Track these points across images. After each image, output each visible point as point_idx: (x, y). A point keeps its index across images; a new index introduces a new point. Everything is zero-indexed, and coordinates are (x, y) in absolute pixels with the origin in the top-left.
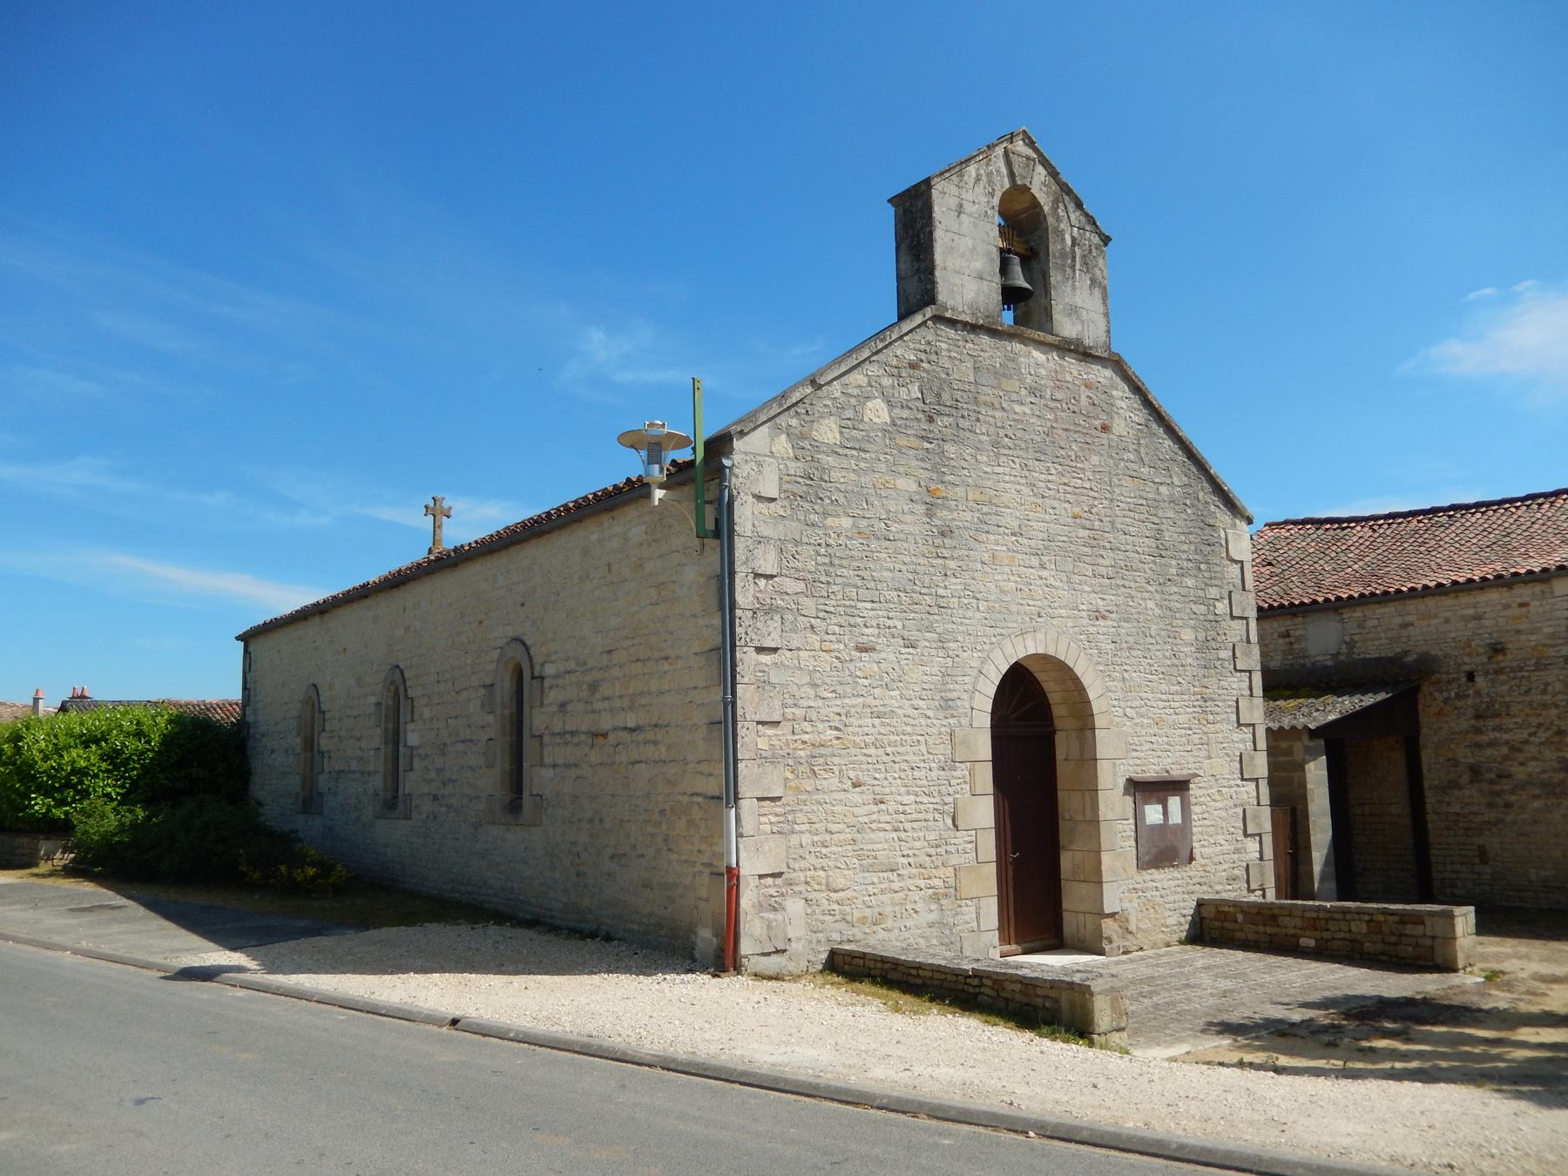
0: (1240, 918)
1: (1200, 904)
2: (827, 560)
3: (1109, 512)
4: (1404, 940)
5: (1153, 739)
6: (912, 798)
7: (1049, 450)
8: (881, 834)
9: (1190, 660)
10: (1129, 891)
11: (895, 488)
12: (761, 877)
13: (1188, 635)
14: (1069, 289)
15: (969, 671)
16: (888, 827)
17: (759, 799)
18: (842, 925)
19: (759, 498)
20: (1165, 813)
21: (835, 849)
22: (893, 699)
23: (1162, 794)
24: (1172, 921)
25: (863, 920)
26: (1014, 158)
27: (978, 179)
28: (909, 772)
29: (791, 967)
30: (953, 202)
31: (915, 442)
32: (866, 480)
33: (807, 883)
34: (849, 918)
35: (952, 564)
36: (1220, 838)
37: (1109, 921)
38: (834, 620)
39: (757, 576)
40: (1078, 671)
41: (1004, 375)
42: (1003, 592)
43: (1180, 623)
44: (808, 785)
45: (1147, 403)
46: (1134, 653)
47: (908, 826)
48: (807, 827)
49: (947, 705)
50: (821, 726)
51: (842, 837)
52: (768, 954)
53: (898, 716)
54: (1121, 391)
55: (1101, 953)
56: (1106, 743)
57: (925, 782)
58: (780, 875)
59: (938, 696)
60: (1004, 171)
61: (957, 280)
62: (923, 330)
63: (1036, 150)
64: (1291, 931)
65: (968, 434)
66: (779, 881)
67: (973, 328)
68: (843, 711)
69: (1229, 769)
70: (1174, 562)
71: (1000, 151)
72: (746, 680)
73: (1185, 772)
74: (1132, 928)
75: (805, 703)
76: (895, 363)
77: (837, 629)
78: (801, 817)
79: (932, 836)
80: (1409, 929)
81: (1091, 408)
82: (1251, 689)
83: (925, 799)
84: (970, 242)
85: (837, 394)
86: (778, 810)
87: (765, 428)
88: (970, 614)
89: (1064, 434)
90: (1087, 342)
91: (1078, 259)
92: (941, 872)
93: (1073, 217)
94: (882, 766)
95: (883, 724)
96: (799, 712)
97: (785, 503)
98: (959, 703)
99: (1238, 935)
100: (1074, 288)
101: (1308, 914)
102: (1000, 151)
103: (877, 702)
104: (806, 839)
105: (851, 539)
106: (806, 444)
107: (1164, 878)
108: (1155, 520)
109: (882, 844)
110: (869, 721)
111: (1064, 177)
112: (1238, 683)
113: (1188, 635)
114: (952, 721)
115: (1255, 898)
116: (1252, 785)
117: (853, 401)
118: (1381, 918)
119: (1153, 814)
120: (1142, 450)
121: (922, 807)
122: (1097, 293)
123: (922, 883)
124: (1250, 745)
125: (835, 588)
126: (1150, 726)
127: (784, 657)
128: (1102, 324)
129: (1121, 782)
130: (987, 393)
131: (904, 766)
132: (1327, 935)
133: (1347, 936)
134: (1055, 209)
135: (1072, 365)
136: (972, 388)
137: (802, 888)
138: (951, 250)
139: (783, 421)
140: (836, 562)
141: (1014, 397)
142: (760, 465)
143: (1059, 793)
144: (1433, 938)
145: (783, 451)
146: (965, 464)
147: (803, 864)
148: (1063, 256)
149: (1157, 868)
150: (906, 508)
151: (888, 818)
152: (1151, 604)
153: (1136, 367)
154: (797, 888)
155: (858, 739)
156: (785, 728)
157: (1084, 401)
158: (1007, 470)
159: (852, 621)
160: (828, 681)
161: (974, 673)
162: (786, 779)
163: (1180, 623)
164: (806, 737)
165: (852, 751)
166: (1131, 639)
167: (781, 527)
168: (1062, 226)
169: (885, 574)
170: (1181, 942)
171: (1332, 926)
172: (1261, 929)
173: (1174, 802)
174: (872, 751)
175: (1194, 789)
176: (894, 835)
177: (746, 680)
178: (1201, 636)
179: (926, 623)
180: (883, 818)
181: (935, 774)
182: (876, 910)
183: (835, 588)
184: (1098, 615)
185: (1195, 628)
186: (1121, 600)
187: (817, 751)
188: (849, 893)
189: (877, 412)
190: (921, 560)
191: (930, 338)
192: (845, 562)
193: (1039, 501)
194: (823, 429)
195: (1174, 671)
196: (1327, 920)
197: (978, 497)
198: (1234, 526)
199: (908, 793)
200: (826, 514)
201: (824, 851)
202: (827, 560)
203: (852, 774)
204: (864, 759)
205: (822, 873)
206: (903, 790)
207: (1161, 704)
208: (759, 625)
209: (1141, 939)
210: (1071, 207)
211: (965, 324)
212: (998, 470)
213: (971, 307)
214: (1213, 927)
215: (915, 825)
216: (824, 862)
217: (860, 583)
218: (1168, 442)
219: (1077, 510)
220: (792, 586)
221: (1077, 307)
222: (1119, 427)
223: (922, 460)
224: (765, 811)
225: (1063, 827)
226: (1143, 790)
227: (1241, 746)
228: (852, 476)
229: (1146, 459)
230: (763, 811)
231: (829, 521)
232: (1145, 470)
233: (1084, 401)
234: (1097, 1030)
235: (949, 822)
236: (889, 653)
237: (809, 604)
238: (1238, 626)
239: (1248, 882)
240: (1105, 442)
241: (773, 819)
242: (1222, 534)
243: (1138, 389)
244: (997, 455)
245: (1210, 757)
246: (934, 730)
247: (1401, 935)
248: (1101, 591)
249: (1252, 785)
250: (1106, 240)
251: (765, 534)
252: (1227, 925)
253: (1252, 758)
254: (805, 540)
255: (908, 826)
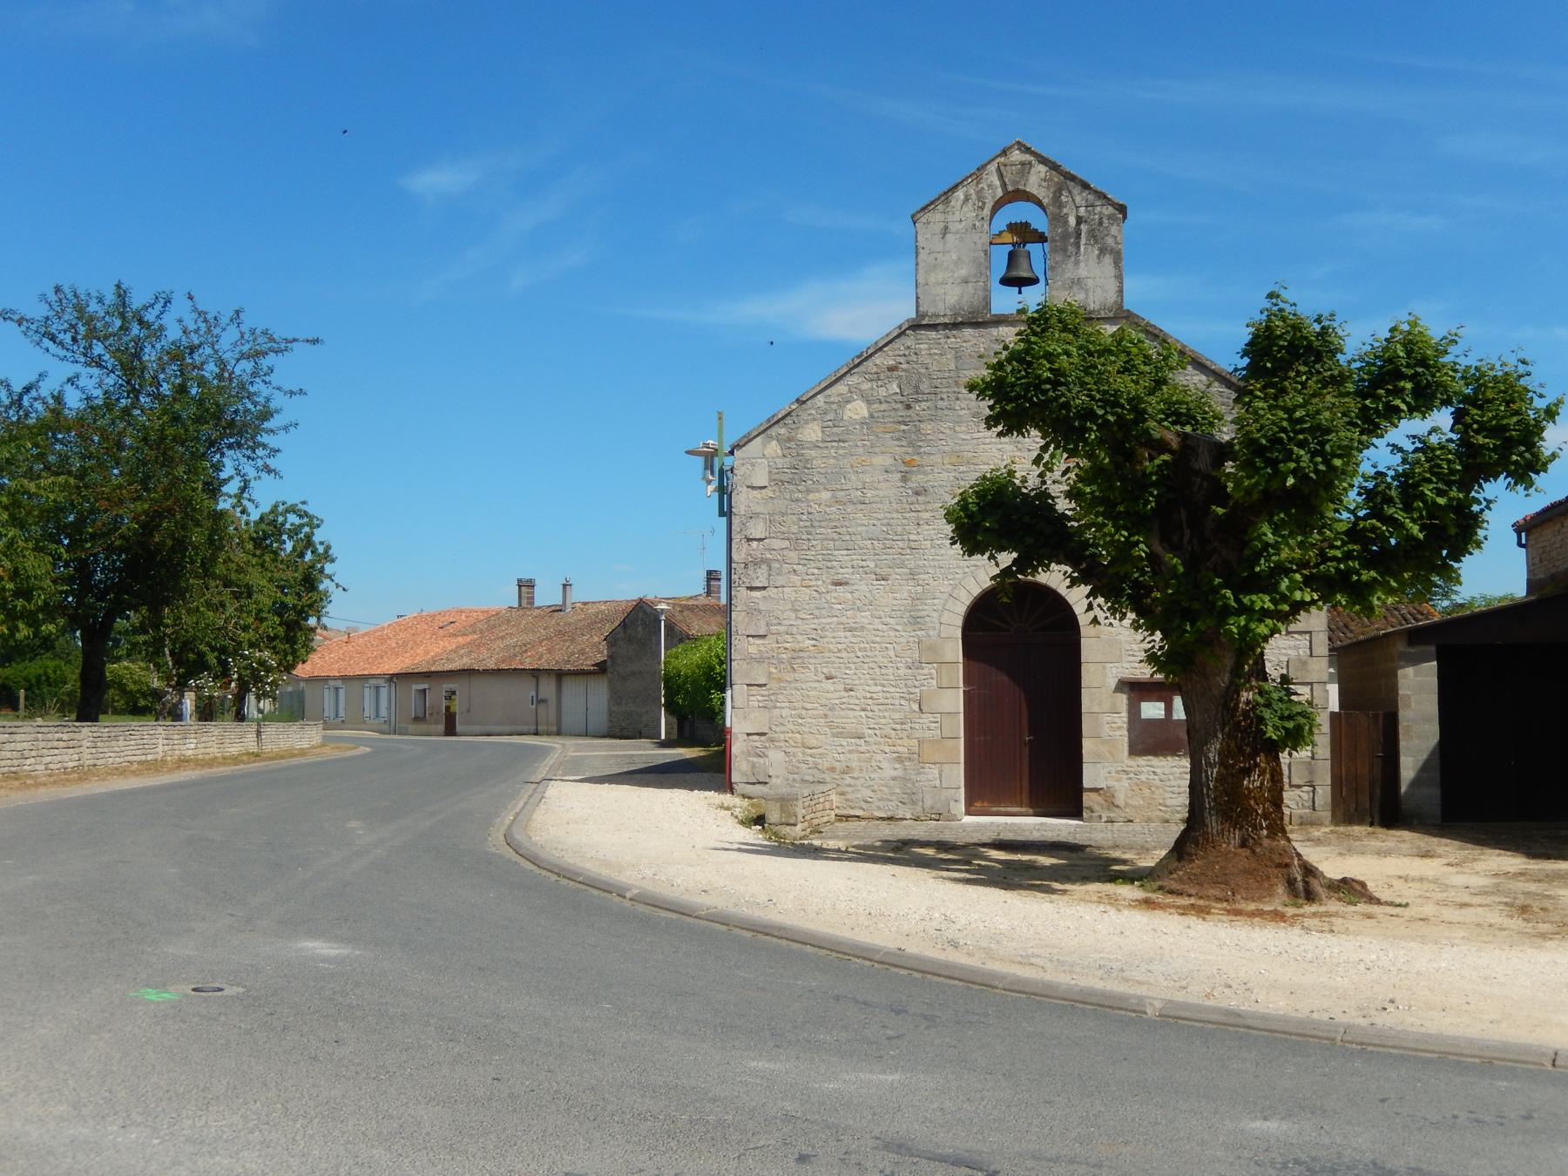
8: (851, 713)
20: (1169, 709)
22: (864, 618)
25: (832, 769)
27: (967, 199)
30: (939, 227)
37: (1093, 796)
39: (749, 540)
49: (916, 621)
50: (800, 638)
62: (903, 340)
67: (956, 326)
71: (992, 167)
74: (1120, 801)
79: (897, 716)
84: (954, 257)
85: (820, 404)
90: (1091, 307)
92: (906, 742)
93: (1078, 199)
96: (781, 629)
100: (1077, 263)
102: (992, 167)
104: (785, 712)
106: (792, 444)
111: (1067, 167)
123: (887, 749)
127: (771, 592)
142: (753, 465)
174: (844, 655)
181: (902, 672)
189: (858, 410)
197: (954, 460)
200: (808, 491)
209: (1129, 813)
210: (1076, 190)
211: (946, 326)
220: (777, 544)
227: (1292, 653)
228: (832, 461)
231: (811, 496)
235: (915, 707)
237: (793, 555)
250: (1122, 209)
253: (1305, 663)
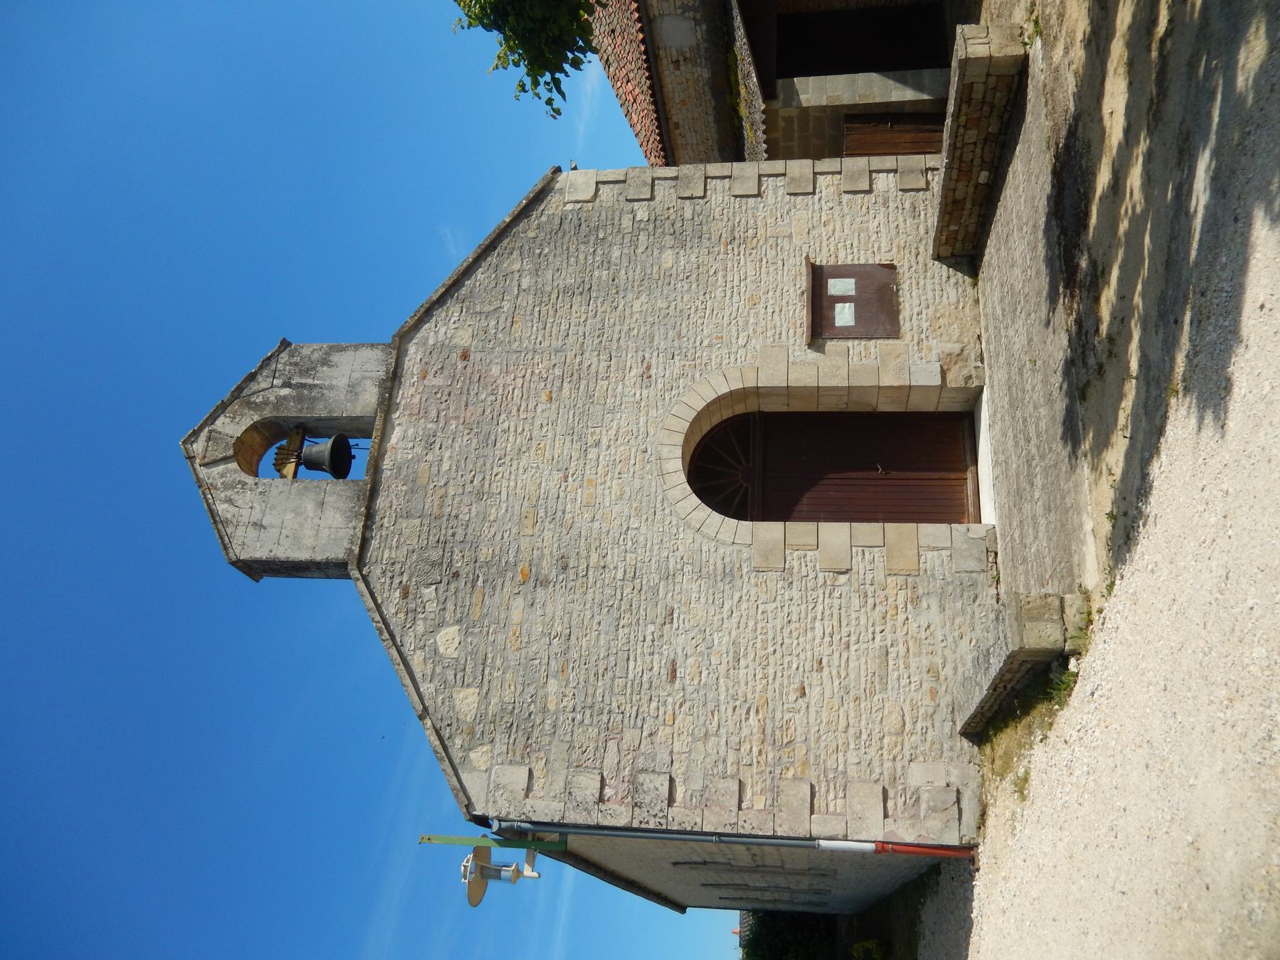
0: (953, 228)
1: (938, 257)
2: (588, 712)
3: (546, 356)
4: (989, 99)
5: (770, 310)
6: (818, 624)
7: (486, 428)
8: (852, 665)
9: (693, 258)
10: (920, 350)
11: (521, 624)
12: (886, 816)
13: (668, 258)
14: (332, 394)
15: (697, 545)
16: (845, 655)
17: (812, 813)
18: (937, 717)
19: (529, 790)
20: (844, 299)
21: (863, 723)
22: (722, 641)
23: (825, 304)
24: (952, 293)
25: (933, 693)
26: (211, 456)
27: (229, 501)
28: (793, 626)
29: (973, 785)
30: (252, 533)
31: (477, 598)
32: (513, 657)
33: (894, 759)
34: (931, 710)
35: (594, 558)
36: (873, 225)
37: (950, 377)
38: (645, 708)
39: (601, 799)
40: (700, 405)
41: (414, 481)
42: (621, 497)
43: (655, 269)
44: (801, 751)
45: (441, 301)
46: (684, 332)
47: (845, 630)
48: (840, 754)
49: (729, 574)
50: (745, 732)
51: (852, 715)
52: (960, 810)
53: (738, 636)
54: (431, 333)
55: (980, 390)
56: (772, 377)
57: (803, 607)
58: (885, 792)
59: (720, 584)
60: (221, 468)
61: (324, 533)
62: (373, 580)
63: (201, 428)
64: (971, 190)
65: (470, 531)
66: (891, 793)
67: (369, 516)
68: (732, 704)
69: (803, 211)
70: (596, 273)
71: (203, 472)
72: (699, 820)
73: (804, 269)
74: (956, 348)
75: (723, 749)
76: (402, 615)
77: (654, 705)
78: (831, 763)
79: (856, 602)
80: (977, 95)
81: (446, 372)
82: (724, 178)
83: (820, 608)
84: (290, 516)
85: (432, 688)
86: (823, 789)
87: (464, 777)
88: (641, 539)
89: (470, 408)
90: (382, 374)
91: (303, 381)
92: (891, 592)
93: (264, 385)
94: (787, 659)
95: (746, 655)
96: (731, 758)
97: (534, 756)
98: (727, 559)
99: (971, 229)
100: (331, 387)
101: (954, 176)
102: (203, 472)
103: (725, 661)
104: (852, 758)
105: (568, 681)
106: (479, 729)
107: (910, 303)
108: (554, 296)
109: (861, 664)
110: (742, 672)
111: (227, 396)
112: (719, 195)
113: (668, 258)
114: (745, 570)
115: (937, 181)
116: (821, 179)
117: (438, 670)
118: (963, 119)
119: (844, 315)
120: (487, 309)
121: (827, 612)
122: (335, 358)
123: (901, 617)
124: (780, 181)
125: (614, 705)
126: (756, 314)
127: (678, 771)
128: (366, 353)
129: (812, 355)
130: (431, 504)
131: (786, 633)
132: (977, 161)
133: (979, 146)
134: (256, 407)
135: (407, 394)
136: (426, 522)
137: (899, 765)
138: (297, 540)
139: (457, 755)
140: (589, 700)
141: (434, 470)
142: (497, 787)
143: (821, 409)
144: (988, 75)
145: (485, 758)
146: (498, 537)
147: (876, 764)
148: (299, 399)
149: (898, 312)
150: (540, 612)
151: (836, 655)
152: (636, 308)
153: (406, 316)
154: (899, 772)
155: (759, 688)
156: (746, 775)
157: (439, 381)
158: (505, 483)
159: (646, 686)
160: (702, 719)
161: (698, 536)
162: (795, 778)
163: (655, 269)
164: (755, 750)
165: (770, 694)
166: (671, 333)
167: (556, 765)
168: (272, 398)
169: (602, 642)
170: (975, 285)
171: (968, 157)
172: (965, 212)
173: (837, 286)
174: (771, 670)
175: (821, 260)
176: (853, 648)
177: (699, 820)
178: (669, 241)
179: (649, 594)
180: (836, 663)
181: (795, 594)
182: (925, 676)
183: (614, 705)
184: (646, 376)
185: (661, 249)
186: (632, 345)
187: (769, 739)
188: (907, 709)
189: (448, 640)
190: (590, 596)
191: (379, 571)
192: (590, 691)
193: (534, 443)
194: (465, 709)
195: (703, 278)
196: (961, 161)
197: (529, 522)
198: (561, 191)
199: (813, 629)
200: (544, 710)
201: (864, 737)
202: (588, 712)
203: (792, 697)
204: (778, 680)
205: (886, 741)
206: (809, 635)
207: (736, 298)
208: (647, 800)
209: (969, 338)
210: (254, 386)
211: (367, 528)
212: (504, 496)
213: (349, 519)
214: (963, 248)
215: (844, 624)
216: (876, 737)
217: (610, 674)
218: (480, 275)
219: (544, 398)
220: (611, 758)
221: (349, 383)
222: (463, 338)
223: (494, 588)
224: (823, 804)
225: (852, 408)
226: (820, 328)
227: (780, 192)
228: (509, 676)
229: (496, 304)
230: (823, 808)
231: (552, 707)
232: (507, 306)
233: (439, 381)
234: (1060, 644)
235: (843, 579)
236: (680, 642)
237: (630, 736)
238: (661, 189)
239: (918, 190)
240: (478, 356)
241: (831, 796)
242: (569, 207)
243: (427, 313)
244: (490, 495)
245: (790, 236)
246: (753, 592)
247: (983, 102)
248: (623, 369)
249: (821, 179)
250: (285, 344)
251: (562, 784)
252: (960, 237)
253: (793, 179)
254: (568, 738)
255: (845, 630)
